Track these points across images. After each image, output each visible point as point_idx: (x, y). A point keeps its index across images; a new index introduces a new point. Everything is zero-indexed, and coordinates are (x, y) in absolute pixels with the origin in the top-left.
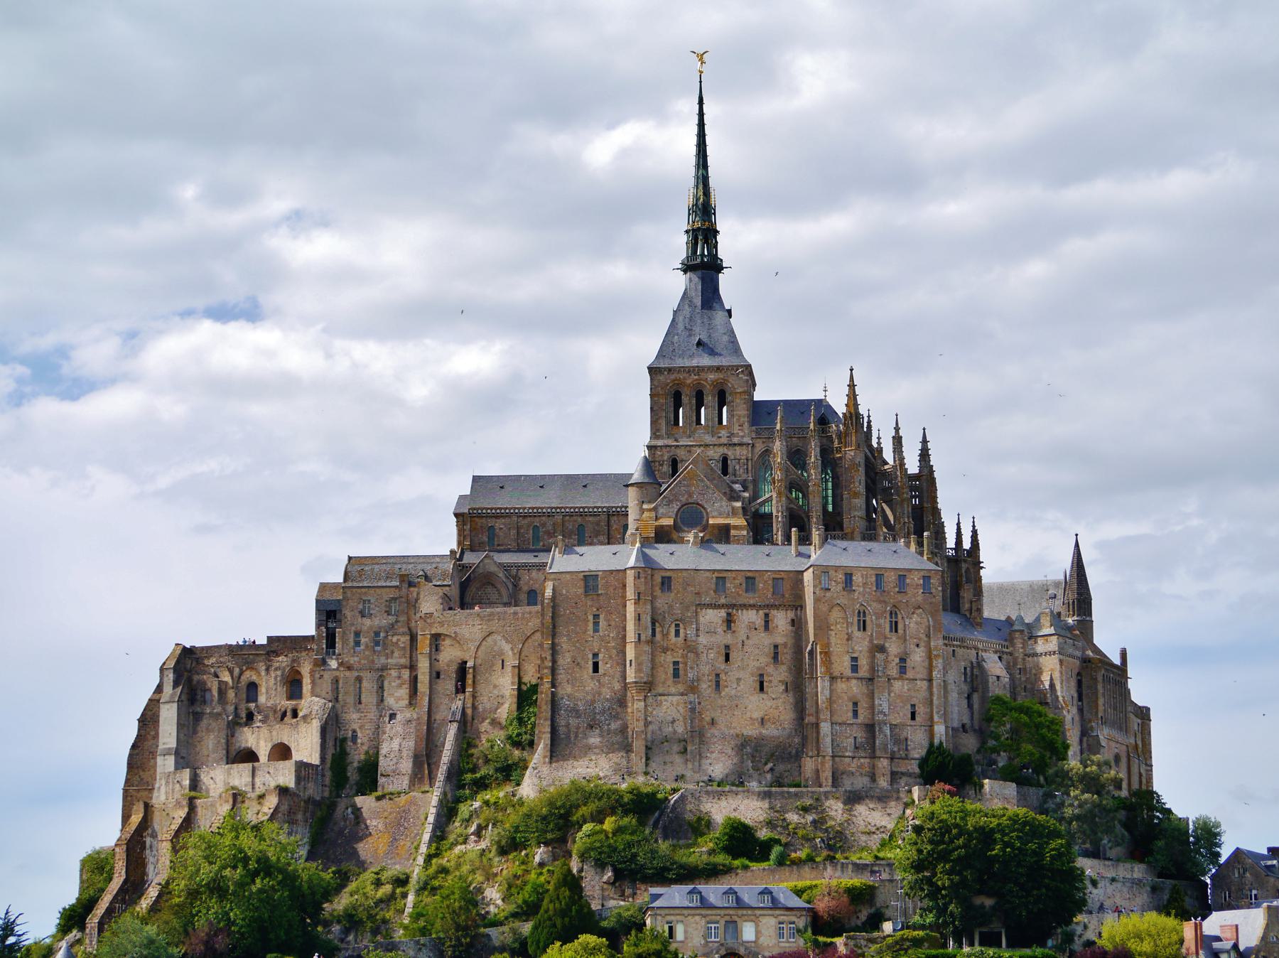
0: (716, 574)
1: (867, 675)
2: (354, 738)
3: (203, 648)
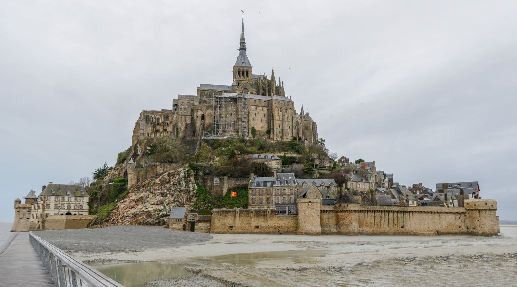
1: (282, 120)
3: (148, 111)
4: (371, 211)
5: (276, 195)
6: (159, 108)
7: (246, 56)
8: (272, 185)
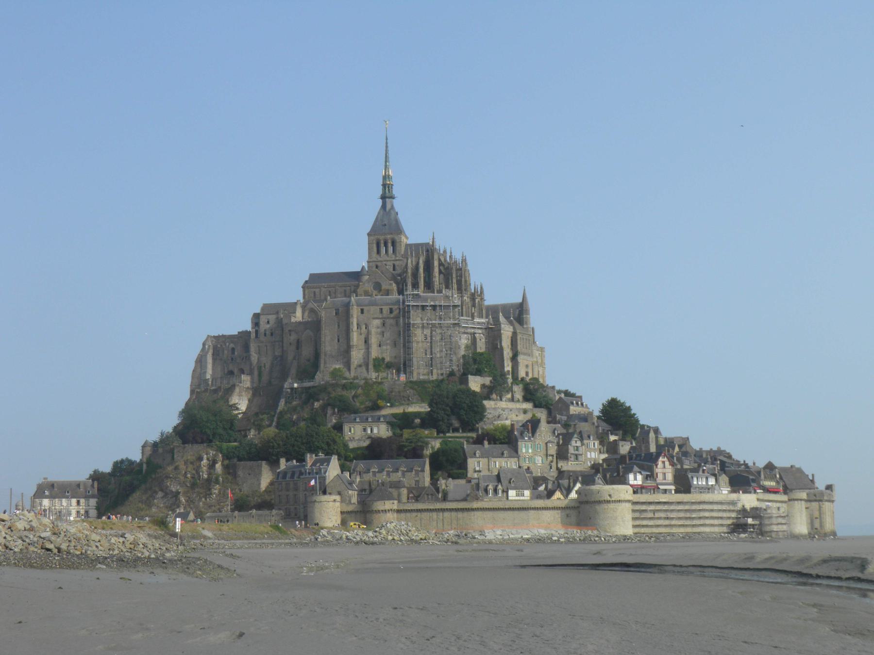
0: (379, 307)
2: (265, 366)
4: (414, 510)
5: (304, 491)
6: (233, 330)
7: (392, 211)
8: (299, 477)
